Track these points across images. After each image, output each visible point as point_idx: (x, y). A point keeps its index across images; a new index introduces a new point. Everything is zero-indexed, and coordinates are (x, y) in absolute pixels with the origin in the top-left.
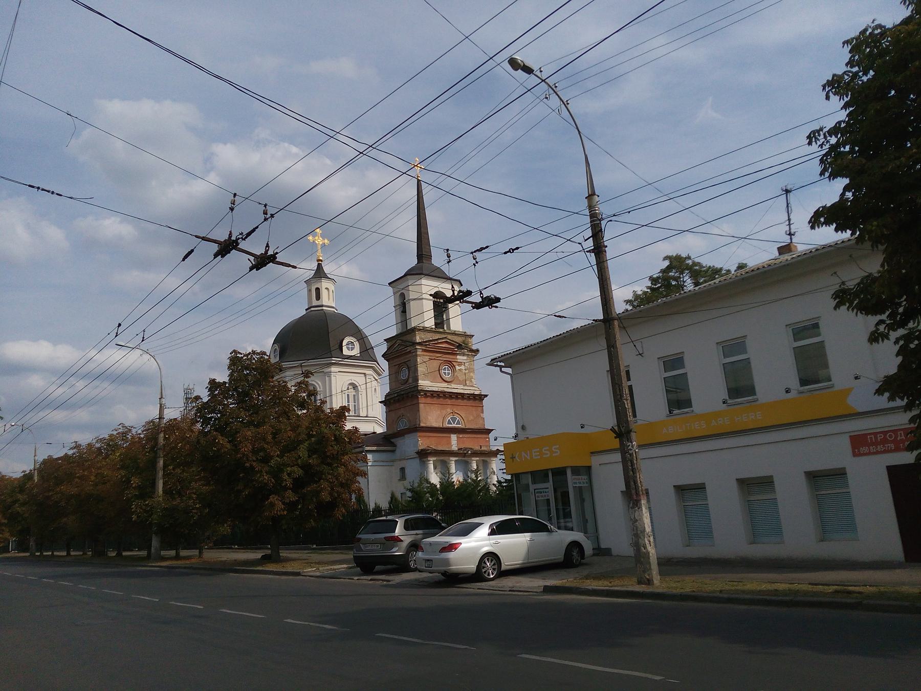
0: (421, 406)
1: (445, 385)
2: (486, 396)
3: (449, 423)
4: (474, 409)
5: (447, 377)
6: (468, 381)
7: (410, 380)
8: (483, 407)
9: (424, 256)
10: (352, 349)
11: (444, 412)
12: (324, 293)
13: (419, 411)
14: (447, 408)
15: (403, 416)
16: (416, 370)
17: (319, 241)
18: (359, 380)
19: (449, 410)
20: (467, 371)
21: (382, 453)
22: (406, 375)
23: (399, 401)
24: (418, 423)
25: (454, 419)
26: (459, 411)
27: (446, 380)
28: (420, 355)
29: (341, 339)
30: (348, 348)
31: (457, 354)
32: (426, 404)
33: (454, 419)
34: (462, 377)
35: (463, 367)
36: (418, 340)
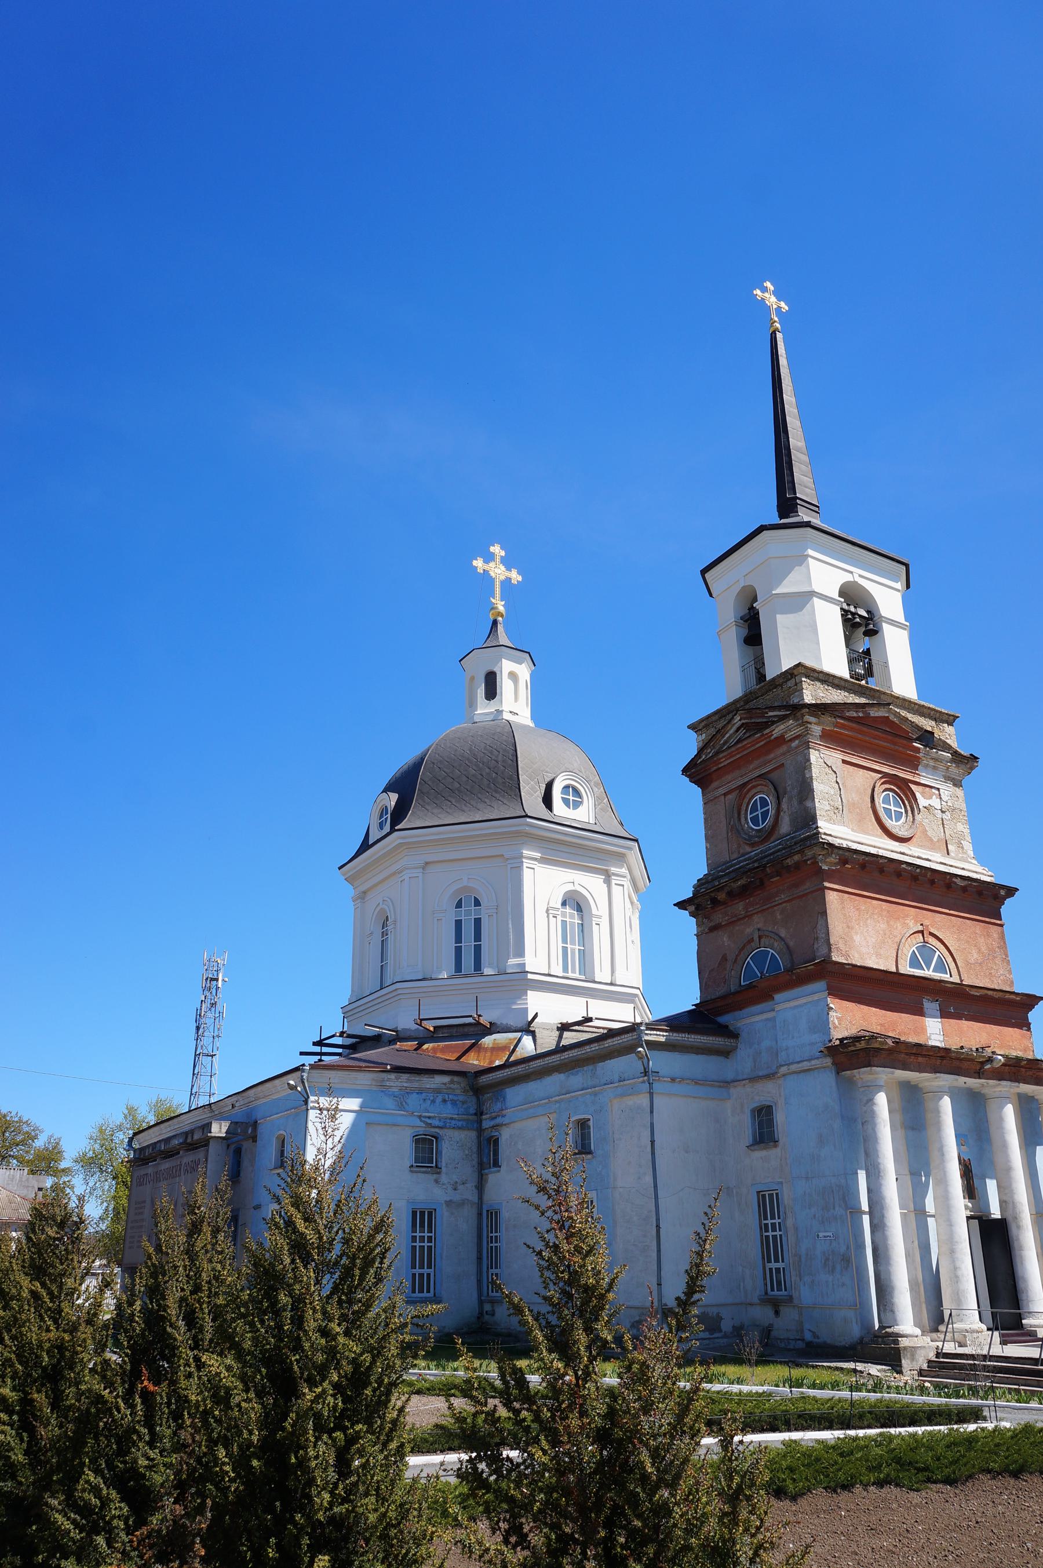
0: (833, 898)
2: (1011, 891)
7: (785, 827)
8: (1002, 925)
9: (798, 501)
10: (577, 805)
12: (505, 686)
13: (824, 913)
15: (760, 937)
16: (806, 790)
17: (498, 571)
18: (590, 884)
21: (693, 1057)
22: (765, 815)
23: (744, 892)
24: (823, 951)
25: (926, 951)
26: (938, 929)
27: (894, 831)
29: (548, 780)
30: (566, 802)
34: (935, 832)
36: (808, 698)
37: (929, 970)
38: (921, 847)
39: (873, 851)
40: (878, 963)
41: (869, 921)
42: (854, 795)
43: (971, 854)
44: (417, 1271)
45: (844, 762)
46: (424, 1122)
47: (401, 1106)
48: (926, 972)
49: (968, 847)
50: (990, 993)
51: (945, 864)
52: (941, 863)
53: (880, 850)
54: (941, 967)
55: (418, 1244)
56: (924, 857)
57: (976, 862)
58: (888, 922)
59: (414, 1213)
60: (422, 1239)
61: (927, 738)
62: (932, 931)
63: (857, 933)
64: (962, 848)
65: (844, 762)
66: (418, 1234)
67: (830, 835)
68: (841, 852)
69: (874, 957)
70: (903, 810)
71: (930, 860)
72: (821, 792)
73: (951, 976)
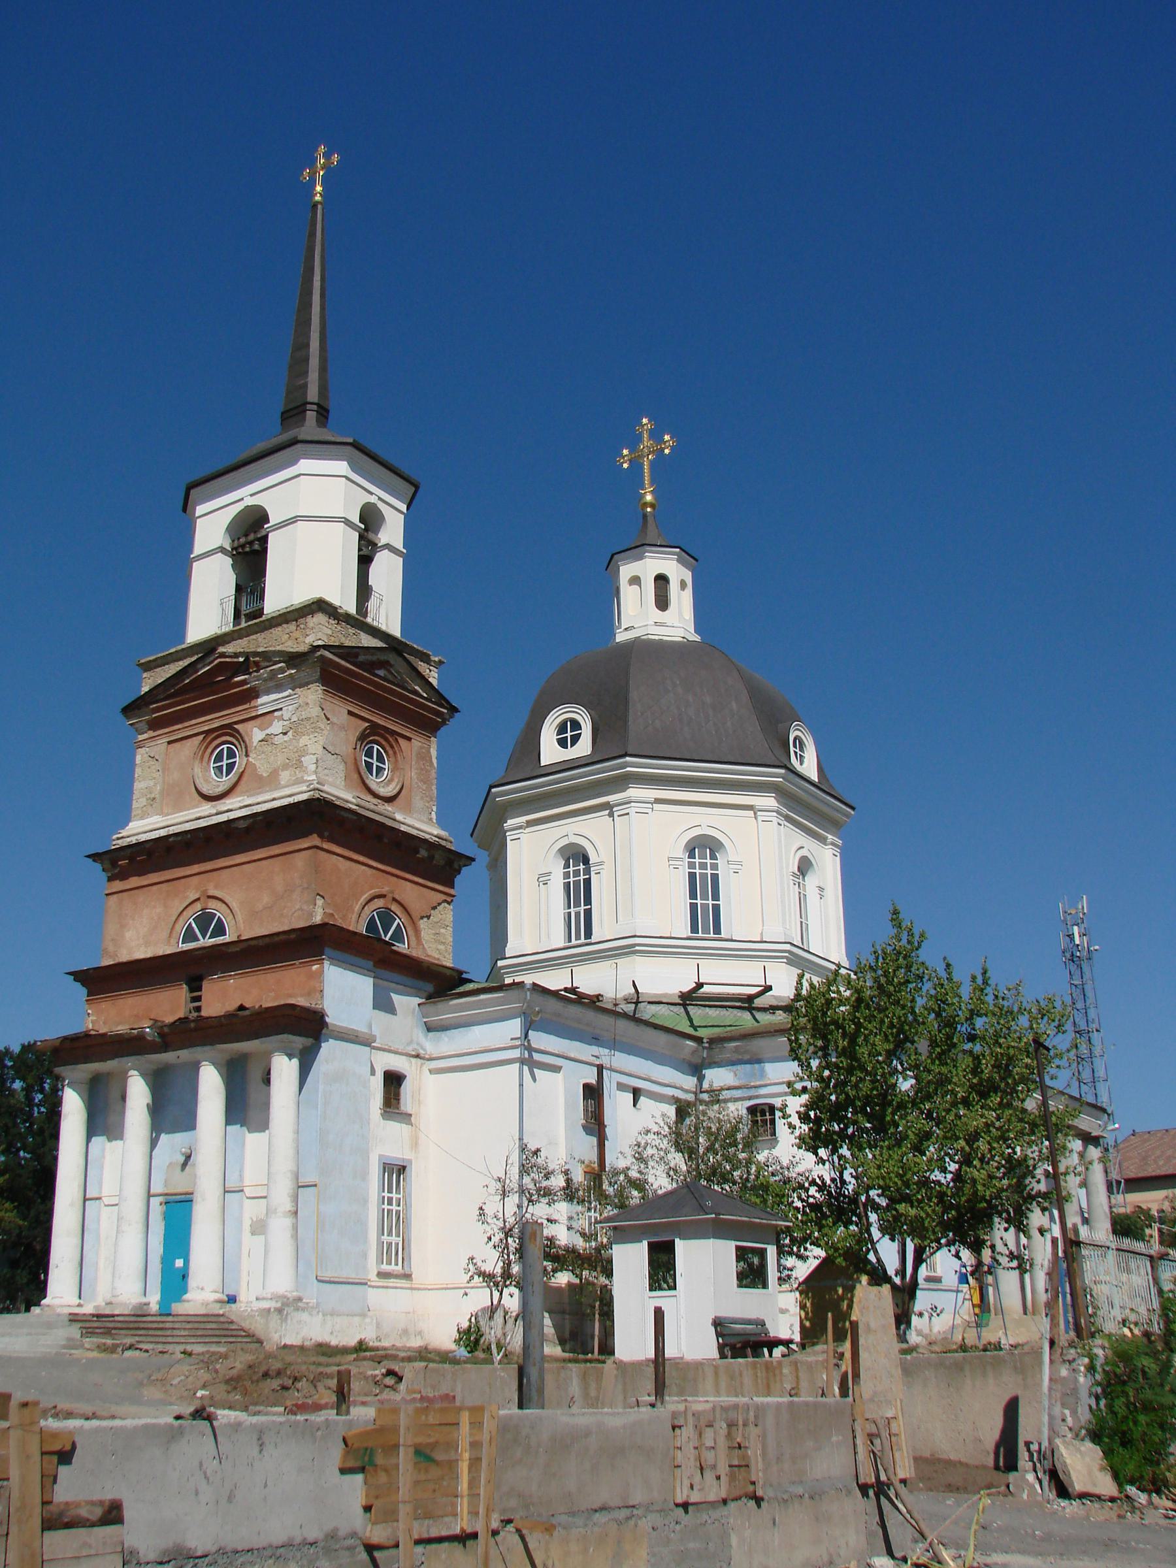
1: (207, 808)
3: (189, 936)
6: (285, 767)
20: (290, 734)
25: (204, 920)
31: (253, 694)
34: (263, 770)
35: (276, 727)
38: (242, 793)
45: (169, 743)
50: (253, 943)
53: (171, 828)
61: (248, 664)
65: (169, 743)
69: (143, 949)
71: (231, 810)
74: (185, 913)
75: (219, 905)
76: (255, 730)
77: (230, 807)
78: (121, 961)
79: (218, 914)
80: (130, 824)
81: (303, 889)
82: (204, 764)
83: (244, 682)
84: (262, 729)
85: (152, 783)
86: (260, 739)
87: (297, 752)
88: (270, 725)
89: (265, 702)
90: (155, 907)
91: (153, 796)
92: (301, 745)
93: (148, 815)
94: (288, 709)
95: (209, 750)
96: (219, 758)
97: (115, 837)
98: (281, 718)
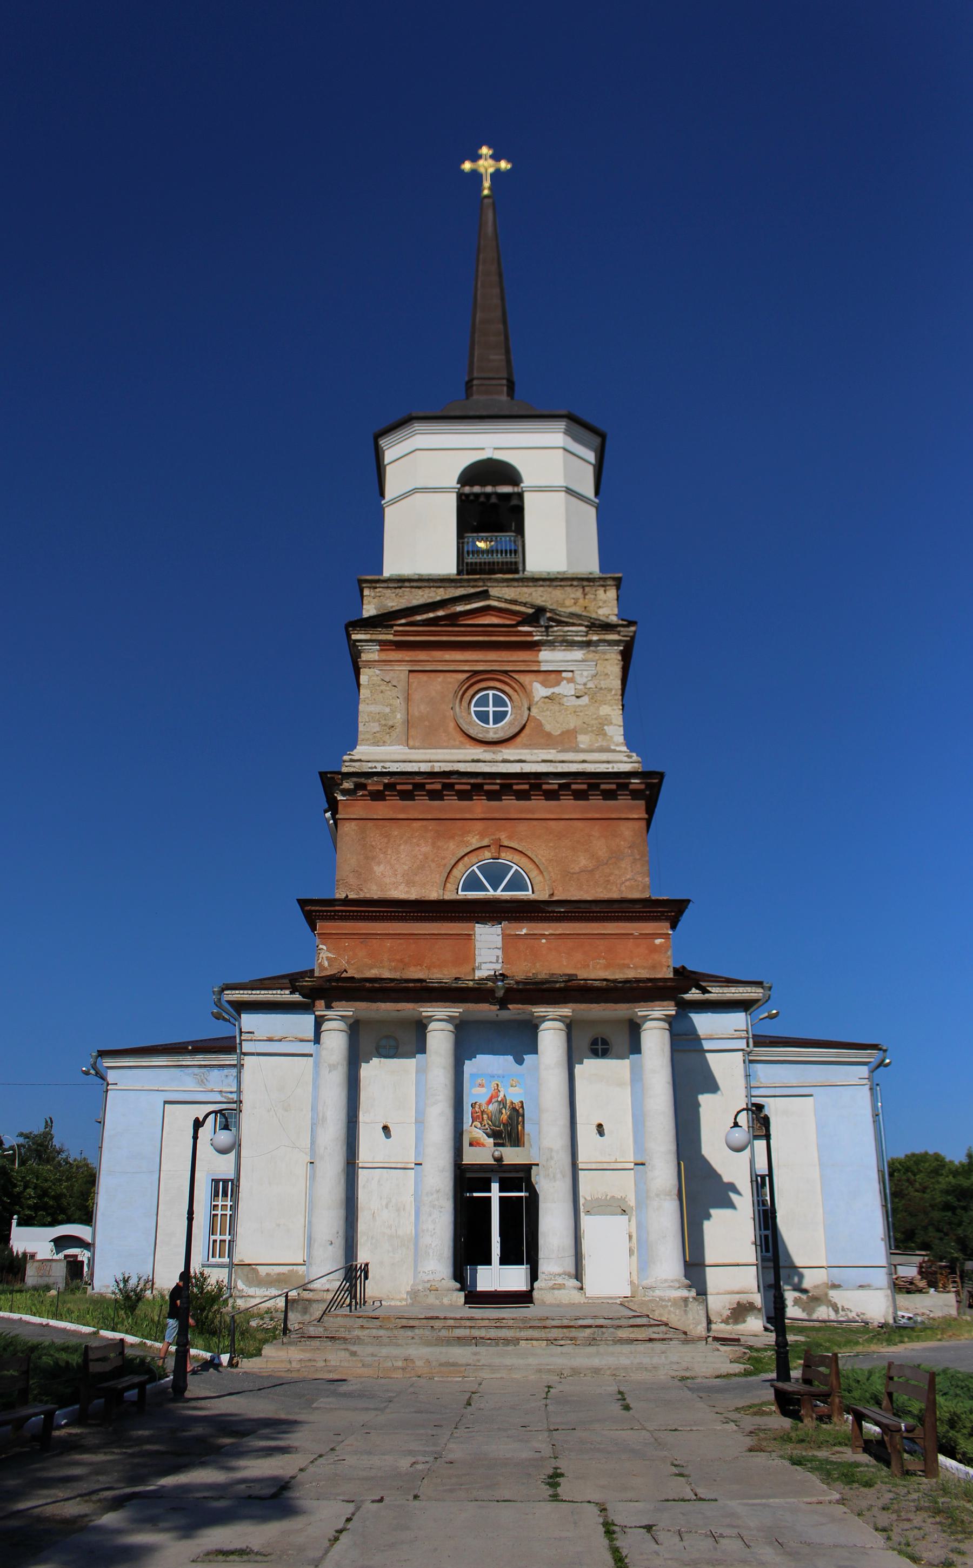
3: (471, 883)
4: (596, 830)
5: (477, 728)
11: (453, 849)
14: (469, 832)
19: (475, 842)
20: (585, 700)
27: (480, 736)
28: (370, 664)
31: (534, 646)
32: (370, 824)
33: (495, 874)
35: (565, 689)
37: (495, 889)
38: (526, 746)
39: (424, 768)
40: (407, 892)
41: (402, 847)
42: (422, 707)
43: (621, 739)
44: (218, 1237)
45: (410, 671)
46: (225, 1097)
47: (202, 1083)
48: (491, 893)
49: (616, 733)
51: (551, 761)
52: (544, 761)
53: (435, 764)
54: (517, 883)
55: (219, 1212)
56: (512, 759)
57: (624, 749)
58: (433, 844)
59: (216, 1182)
60: (224, 1207)
62: (506, 844)
63: (379, 864)
64: (605, 735)
66: (220, 1203)
67: (360, 761)
68: (355, 779)
69: (402, 887)
70: (509, 709)
72: (370, 713)
73: (533, 892)
74: (466, 858)
75: (517, 858)
76: (537, 686)
77: (523, 758)
78: (368, 896)
79: (515, 867)
80: (358, 747)
81: (635, 859)
82: (465, 703)
83: (530, 634)
84: (545, 684)
85: (387, 710)
86: (545, 695)
87: (596, 719)
88: (558, 684)
89: (549, 658)
90: (418, 845)
91: (391, 723)
92: (601, 713)
93: (384, 743)
94: (582, 674)
95: (471, 692)
96: (483, 702)
97: (346, 758)
98: (571, 680)
